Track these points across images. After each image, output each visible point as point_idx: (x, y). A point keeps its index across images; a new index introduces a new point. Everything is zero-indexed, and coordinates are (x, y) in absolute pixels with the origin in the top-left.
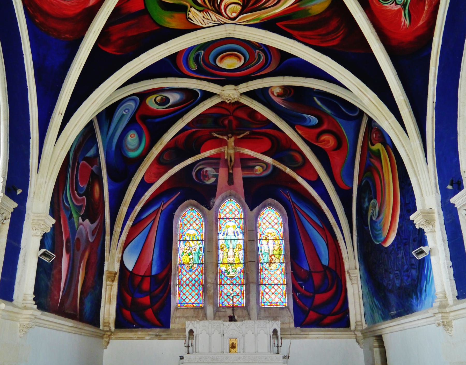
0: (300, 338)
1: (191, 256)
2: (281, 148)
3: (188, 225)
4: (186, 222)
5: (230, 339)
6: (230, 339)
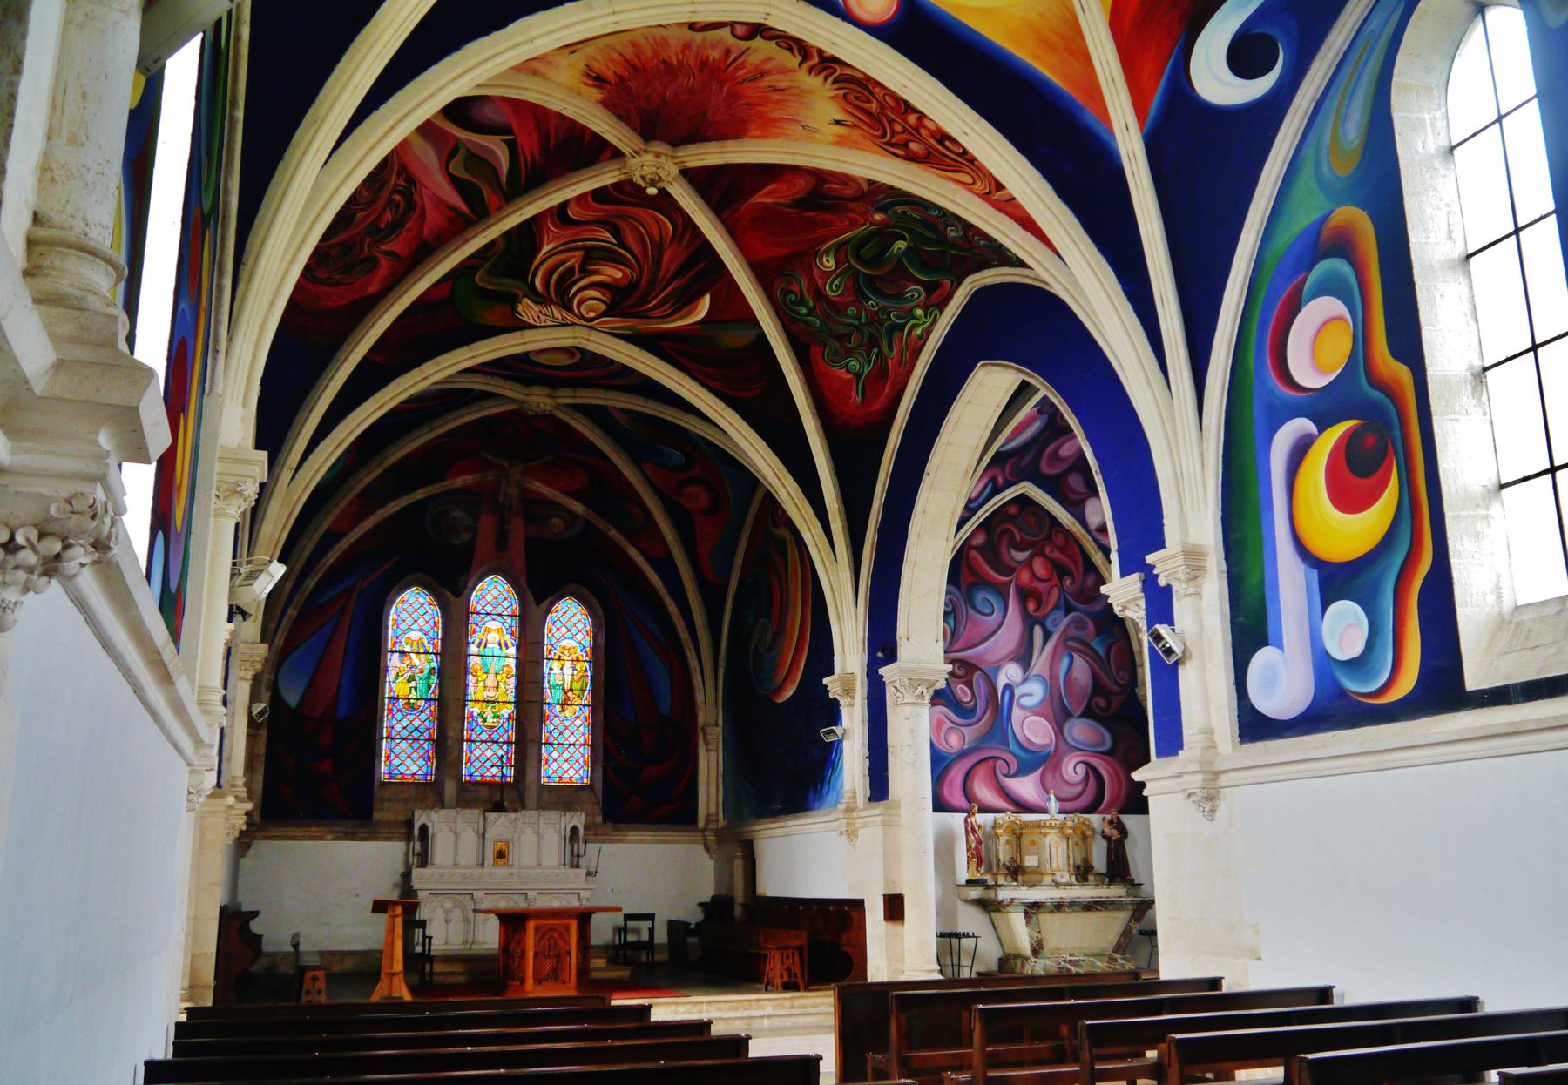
0: (612, 841)
1: (413, 684)
2: (604, 489)
3: (410, 621)
4: (404, 615)
5: (495, 843)
6: (495, 843)
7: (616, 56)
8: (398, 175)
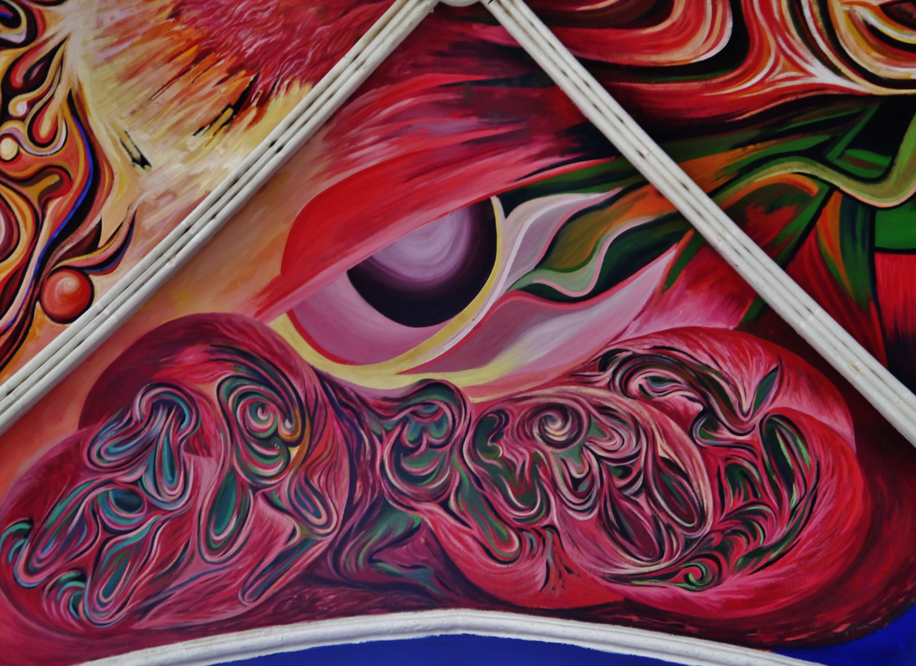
7: (176, 88)
8: (588, 383)
